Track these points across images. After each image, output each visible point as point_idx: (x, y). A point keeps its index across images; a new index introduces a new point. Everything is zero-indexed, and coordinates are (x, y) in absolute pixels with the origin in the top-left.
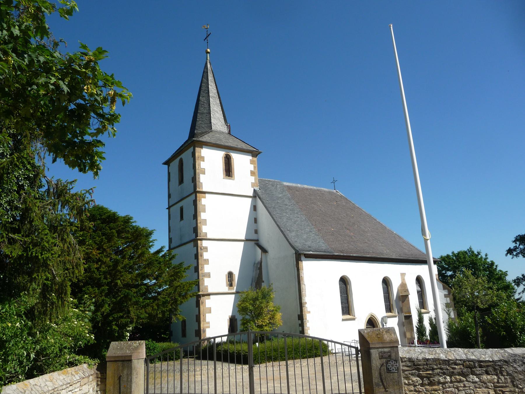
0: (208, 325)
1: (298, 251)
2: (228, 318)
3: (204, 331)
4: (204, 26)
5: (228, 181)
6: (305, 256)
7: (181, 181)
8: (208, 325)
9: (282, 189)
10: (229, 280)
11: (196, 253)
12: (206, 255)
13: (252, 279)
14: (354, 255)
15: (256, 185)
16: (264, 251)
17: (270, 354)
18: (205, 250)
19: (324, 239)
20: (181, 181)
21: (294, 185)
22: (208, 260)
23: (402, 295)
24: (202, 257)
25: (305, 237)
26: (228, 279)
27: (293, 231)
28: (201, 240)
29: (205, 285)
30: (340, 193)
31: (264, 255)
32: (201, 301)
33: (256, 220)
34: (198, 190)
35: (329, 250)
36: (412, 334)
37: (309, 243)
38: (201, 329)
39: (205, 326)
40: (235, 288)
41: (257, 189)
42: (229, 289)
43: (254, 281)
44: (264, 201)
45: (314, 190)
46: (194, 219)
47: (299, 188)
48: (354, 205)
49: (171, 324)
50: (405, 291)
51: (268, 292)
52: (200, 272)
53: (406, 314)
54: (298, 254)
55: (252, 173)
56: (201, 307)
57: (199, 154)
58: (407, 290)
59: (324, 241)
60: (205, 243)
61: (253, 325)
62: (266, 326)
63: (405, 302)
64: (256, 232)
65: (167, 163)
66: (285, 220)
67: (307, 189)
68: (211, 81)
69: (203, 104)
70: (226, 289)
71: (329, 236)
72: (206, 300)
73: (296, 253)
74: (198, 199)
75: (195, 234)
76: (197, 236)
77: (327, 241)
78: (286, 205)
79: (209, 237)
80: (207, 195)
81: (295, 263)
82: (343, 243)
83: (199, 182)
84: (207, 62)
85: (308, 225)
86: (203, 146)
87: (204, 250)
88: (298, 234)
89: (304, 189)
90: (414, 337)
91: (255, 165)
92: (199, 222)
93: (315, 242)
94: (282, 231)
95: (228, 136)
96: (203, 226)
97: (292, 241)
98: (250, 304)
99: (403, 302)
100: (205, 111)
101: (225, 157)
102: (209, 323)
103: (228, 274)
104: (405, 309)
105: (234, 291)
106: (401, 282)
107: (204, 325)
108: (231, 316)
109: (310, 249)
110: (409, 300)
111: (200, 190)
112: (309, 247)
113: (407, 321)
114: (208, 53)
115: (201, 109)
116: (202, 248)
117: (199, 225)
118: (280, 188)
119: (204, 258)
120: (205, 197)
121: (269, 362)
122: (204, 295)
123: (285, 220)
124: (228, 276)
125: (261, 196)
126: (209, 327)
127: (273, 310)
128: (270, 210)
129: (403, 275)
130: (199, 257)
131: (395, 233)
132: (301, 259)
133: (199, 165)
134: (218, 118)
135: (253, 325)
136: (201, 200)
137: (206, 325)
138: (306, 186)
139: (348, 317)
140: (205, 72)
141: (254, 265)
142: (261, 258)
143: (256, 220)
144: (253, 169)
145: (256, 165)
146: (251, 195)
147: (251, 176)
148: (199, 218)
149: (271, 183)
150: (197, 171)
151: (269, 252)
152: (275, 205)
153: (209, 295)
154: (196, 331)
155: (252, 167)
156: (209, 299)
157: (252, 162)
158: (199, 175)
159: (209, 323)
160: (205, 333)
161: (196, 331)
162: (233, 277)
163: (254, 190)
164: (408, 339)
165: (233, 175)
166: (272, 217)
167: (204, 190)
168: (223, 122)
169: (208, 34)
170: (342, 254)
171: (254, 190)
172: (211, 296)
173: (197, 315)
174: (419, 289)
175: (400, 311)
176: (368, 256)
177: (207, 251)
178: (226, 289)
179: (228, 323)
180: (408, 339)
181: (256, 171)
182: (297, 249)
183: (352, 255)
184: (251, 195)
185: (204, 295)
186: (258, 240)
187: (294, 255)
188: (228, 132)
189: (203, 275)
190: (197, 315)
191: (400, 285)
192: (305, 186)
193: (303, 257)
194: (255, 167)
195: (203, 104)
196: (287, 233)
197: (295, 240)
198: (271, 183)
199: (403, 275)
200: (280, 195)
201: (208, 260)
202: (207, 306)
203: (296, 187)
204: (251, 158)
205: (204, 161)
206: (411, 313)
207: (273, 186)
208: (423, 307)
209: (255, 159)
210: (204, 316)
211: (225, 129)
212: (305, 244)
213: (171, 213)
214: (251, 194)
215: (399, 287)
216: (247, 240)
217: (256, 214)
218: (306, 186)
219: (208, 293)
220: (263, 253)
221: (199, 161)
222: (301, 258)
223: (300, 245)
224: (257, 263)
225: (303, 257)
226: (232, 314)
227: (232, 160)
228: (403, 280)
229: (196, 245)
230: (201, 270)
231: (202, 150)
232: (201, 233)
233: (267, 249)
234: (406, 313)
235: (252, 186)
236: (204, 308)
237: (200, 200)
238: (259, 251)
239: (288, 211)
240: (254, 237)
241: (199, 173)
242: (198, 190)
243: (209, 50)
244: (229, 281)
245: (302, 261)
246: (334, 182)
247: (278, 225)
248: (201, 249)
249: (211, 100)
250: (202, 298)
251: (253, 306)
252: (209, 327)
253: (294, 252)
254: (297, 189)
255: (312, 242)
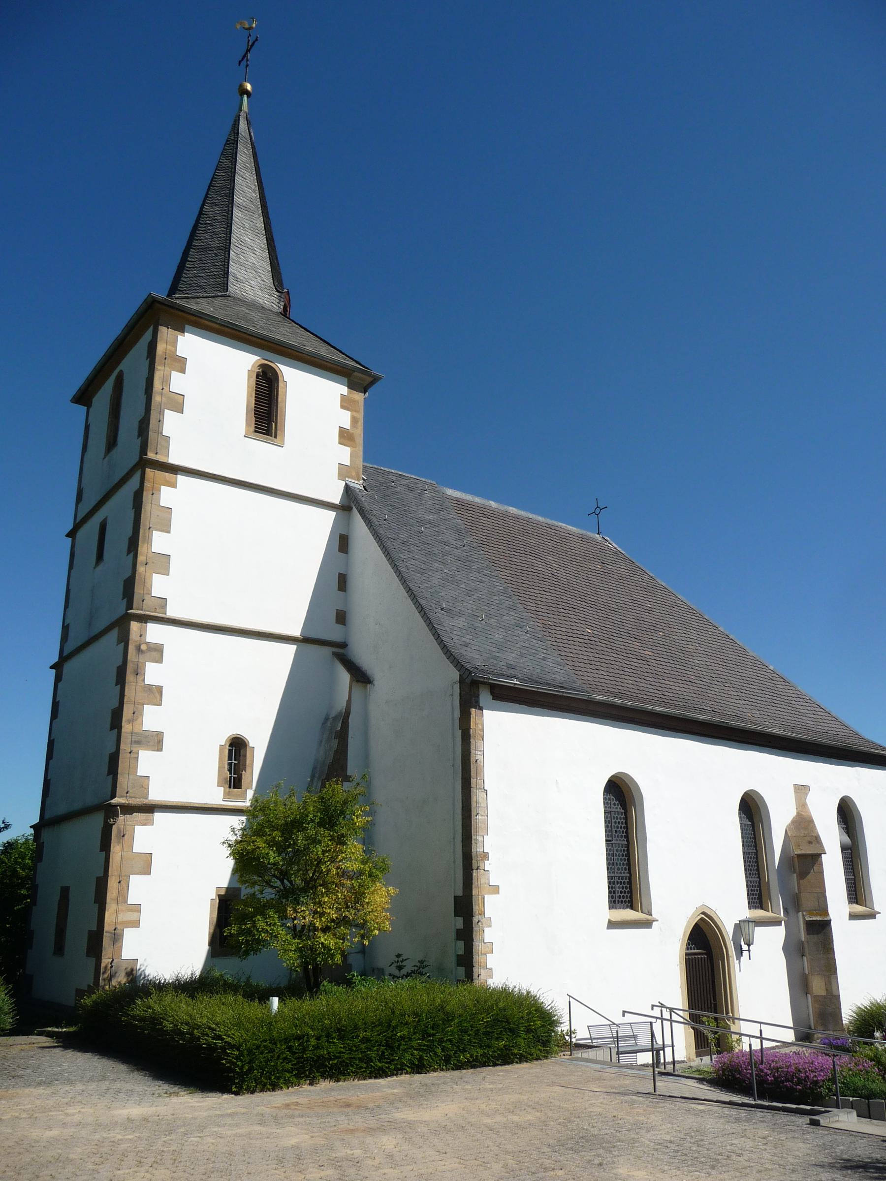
0: (132, 916)
1: (471, 672)
2: (214, 896)
3: (117, 938)
4: (241, 23)
5: (261, 447)
6: (492, 693)
7: (112, 443)
8: (132, 916)
9: (437, 502)
10: (230, 764)
11: (120, 663)
12: (153, 674)
13: (314, 768)
14: (658, 709)
15: (354, 474)
16: (361, 677)
17: (317, 1047)
18: (154, 654)
19: (563, 653)
20: (112, 443)
21: (478, 500)
22: (160, 689)
23: (799, 853)
24: (140, 678)
25: (498, 636)
26: (226, 761)
27: (460, 614)
28: (144, 619)
29: (140, 772)
30: (614, 544)
31: (358, 690)
32: (119, 831)
33: (343, 582)
34: (151, 455)
35: (574, 685)
36: (830, 983)
37: (511, 657)
38: (106, 928)
39: (120, 919)
40: (250, 794)
41: (357, 485)
42: (227, 796)
43: (317, 775)
44: (374, 519)
45: (538, 523)
46: (129, 553)
47: (494, 511)
48: (654, 580)
49: (34, 907)
50: (810, 843)
51: (345, 803)
52: (126, 728)
53: (811, 914)
54: (468, 681)
55: (345, 436)
56: (116, 849)
57: (169, 347)
58: (817, 840)
59: (559, 660)
60: (154, 633)
61: (274, 925)
62: (325, 930)
63: (809, 877)
64: (342, 618)
65: (83, 397)
66: (435, 581)
67: (517, 518)
68: (245, 167)
69: (211, 225)
70: (216, 795)
71: (578, 648)
72: (138, 829)
73: (462, 681)
74: (147, 485)
75: (125, 600)
76: (130, 606)
77: (568, 659)
78: (446, 544)
79: (172, 612)
80: (181, 479)
81: (457, 714)
82: (622, 672)
83: (159, 432)
84: (239, 116)
85: (512, 608)
86: (187, 327)
87: (148, 654)
88: (476, 625)
89: (506, 516)
90: (835, 993)
91: (355, 414)
92: (141, 558)
93: (532, 658)
94: (421, 610)
95: (281, 318)
96: (154, 575)
97: (454, 641)
98: (271, 844)
99: (803, 875)
100: (216, 243)
101: (258, 376)
102: (137, 908)
103: (231, 745)
104: (808, 901)
105: (247, 803)
106: (793, 813)
107: (117, 917)
108: (228, 889)
109: (511, 672)
110: (821, 872)
111: (160, 458)
112: (510, 667)
113: (815, 938)
114: (244, 92)
115: (204, 238)
116: (143, 647)
117: (140, 569)
118: (433, 498)
119: (147, 682)
120: (174, 485)
121: (311, 1084)
122: (129, 809)
123: (435, 581)
124: (230, 751)
125: (367, 506)
126: (136, 924)
127: (361, 873)
128: (389, 544)
129: (801, 790)
130: (130, 677)
131: (771, 667)
132: (477, 702)
133: (167, 380)
134: (254, 268)
135: (274, 925)
136: (160, 490)
137: (124, 917)
138: (513, 510)
139: (858, 909)
140: (232, 142)
141: (324, 723)
142: (349, 702)
143: (345, 582)
144: (347, 426)
145: (360, 416)
146: (337, 501)
147: (340, 443)
148: (142, 549)
149: (405, 482)
150: (156, 398)
151: (376, 683)
152: (410, 537)
153: (151, 809)
154: (90, 932)
155: (345, 419)
156: (151, 823)
157: (346, 403)
158: (161, 413)
159: (137, 908)
160: (117, 945)
161: (90, 932)
162: (245, 756)
163: (347, 488)
164: (816, 999)
165: (278, 432)
166: (395, 567)
167: (174, 459)
168: (269, 281)
169: (250, 43)
170: (619, 701)
171: (347, 489)
172: (158, 816)
173: (98, 879)
174: (847, 839)
175: (794, 904)
176: (701, 717)
177: (160, 660)
178: (216, 795)
179: (211, 914)
180: (816, 999)
181: (359, 432)
182: (468, 666)
183: (650, 707)
184: (337, 501)
185: (129, 809)
186: (344, 645)
187: (457, 687)
188: (281, 310)
189: (135, 738)
190: (98, 879)
191: (794, 822)
192: (511, 508)
193: (485, 696)
194: (354, 421)
195: (211, 225)
196: (437, 615)
197: (463, 639)
198: (405, 482)
199: (801, 790)
200: (431, 517)
201: (160, 689)
202: (136, 849)
203: (484, 507)
204: (344, 390)
205: (183, 371)
206: (828, 915)
207: (411, 490)
208: (856, 898)
209: (359, 397)
210: (123, 883)
211: (269, 299)
212: (496, 658)
213: (76, 549)
214: (335, 496)
215: (789, 826)
216: (305, 640)
217: (347, 564)
218: (514, 509)
219: (145, 801)
220: (354, 684)
221: (167, 368)
222: (478, 696)
223: (477, 656)
224: (335, 718)
225: (485, 696)
226: (229, 885)
227: (281, 384)
228: (802, 805)
229: (124, 639)
230: (129, 722)
231: (180, 338)
232: (146, 597)
233: (369, 672)
234: (811, 913)
235: (341, 476)
236: (124, 854)
237: (155, 492)
238: (344, 677)
239: (449, 559)
240: (334, 633)
241: (160, 404)
242: (151, 455)
243: (249, 87)
244: (230, 771)
245: (481, 709)
246: (597, 511)
247: (409, 590)
248: (138, 649)
249: (237, 213)
250: (121, 818)
251: (281, 849)
252: (136, 924)
253: (455, 675)
254: (485, 512)
255: (522, 655)
